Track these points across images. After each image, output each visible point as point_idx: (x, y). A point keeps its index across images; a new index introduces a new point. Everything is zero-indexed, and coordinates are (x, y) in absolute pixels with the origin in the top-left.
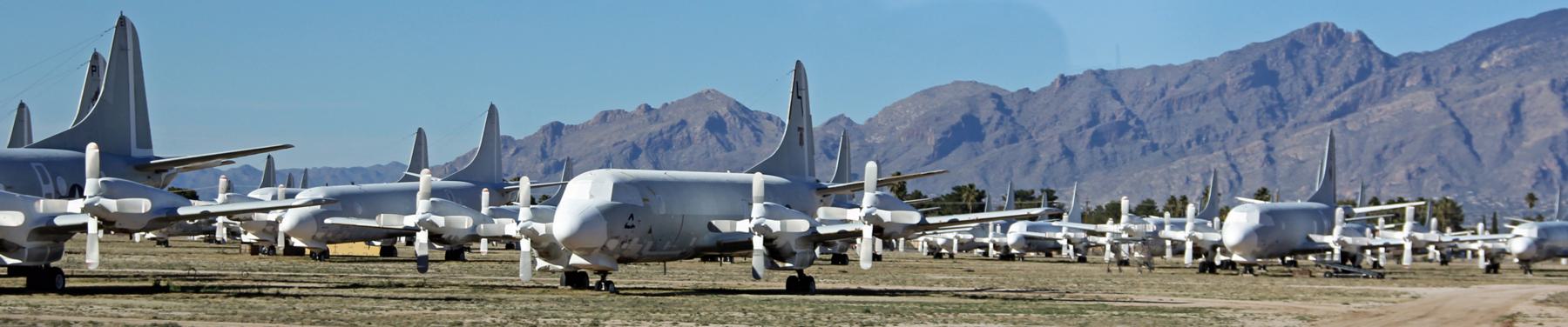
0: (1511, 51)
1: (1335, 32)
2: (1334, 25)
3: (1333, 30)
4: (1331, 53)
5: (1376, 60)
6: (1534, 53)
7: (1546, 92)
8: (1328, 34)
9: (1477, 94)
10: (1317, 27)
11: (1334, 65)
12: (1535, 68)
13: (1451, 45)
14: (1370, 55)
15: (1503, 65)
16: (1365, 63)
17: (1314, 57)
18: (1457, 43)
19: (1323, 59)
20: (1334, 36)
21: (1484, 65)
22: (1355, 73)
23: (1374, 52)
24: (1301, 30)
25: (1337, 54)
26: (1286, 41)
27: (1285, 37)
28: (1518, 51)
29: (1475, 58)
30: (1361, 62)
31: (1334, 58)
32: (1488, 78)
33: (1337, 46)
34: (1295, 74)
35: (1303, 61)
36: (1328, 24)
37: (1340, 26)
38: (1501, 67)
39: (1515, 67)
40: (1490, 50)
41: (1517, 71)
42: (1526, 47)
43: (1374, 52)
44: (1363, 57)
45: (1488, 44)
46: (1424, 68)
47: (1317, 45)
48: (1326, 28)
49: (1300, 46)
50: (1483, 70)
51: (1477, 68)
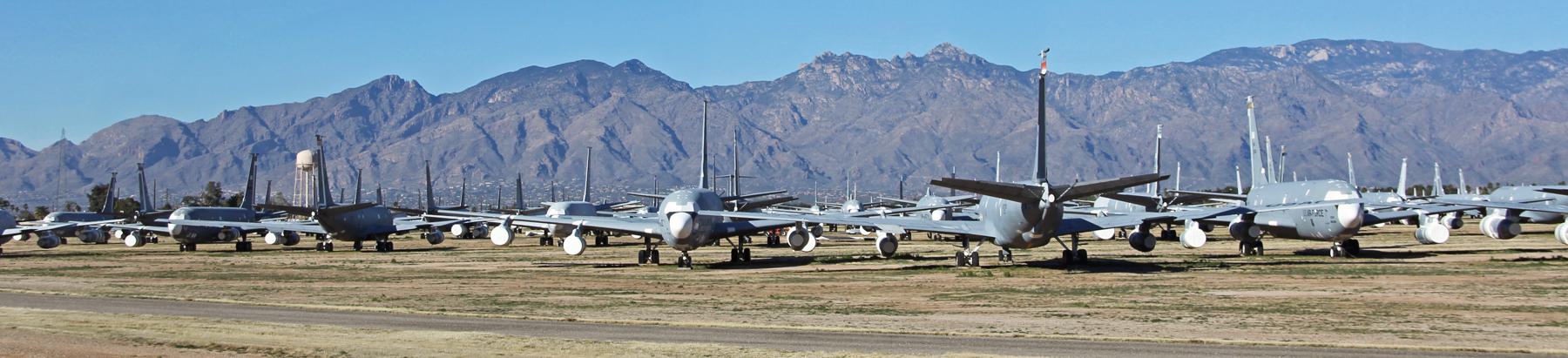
4: (398, 94)
5: (426, 99)
8: (396, 83)
9: (493, 119)
10: (388, 77)
11: (400, 102)
12: (525, 103)
13: (469, 89)
14: (422, 95)
16: (419, 100)
17: (387, 97)
20: (399, 84)
21: (491, 101)
22: (414, 106)
23: (424, 93)
24: (378, 80)
25: (401, 95)
26: (369, 87)
27: (368, 85)
28: (510, 93)
29: (484, 97)
30: (417, 99)
31: (399, 97)
32: (497, 109)
34: (376, 108)
35: (380, 100)
39: (513, 102)
40: (493, 91)
42: (515, 90)
43: (424, 93)
44: (418, 96)
45: (491, 89)
46: (459, 104)
48: (393, 79)
49: (380, 91)
50: (493, 104)
51: (486, 103)
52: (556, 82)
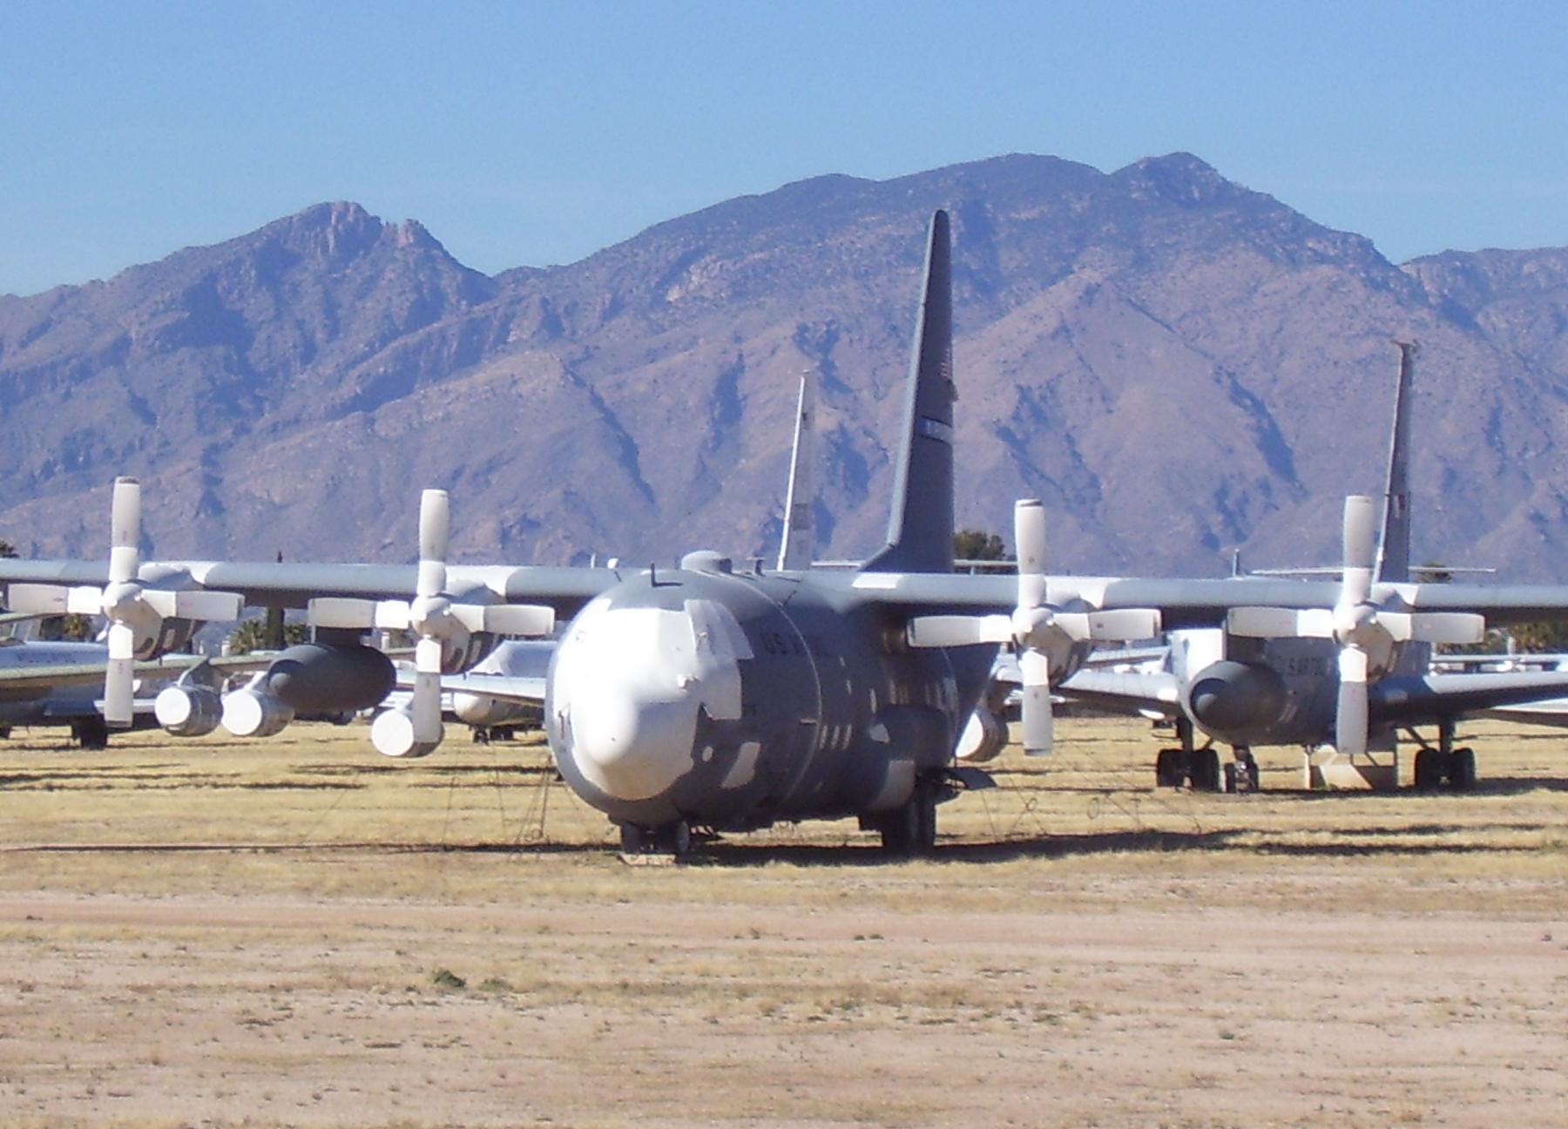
0: (728, 264)
1: (362, 225)
2: (359, 208)
3: (357, 219)
6: (769, 269)
7: (788, 353)
12: (769, 301)
15: (708, 294)
18: (617, 247)
19: (336, 281)
21: (674, 295)
32: (674, 323)
33: (366, 254)
36: (346, 205)
37: (371, 211)
38: (703, 299)
40: (684, 263)
41: (734, 307)
47: (325, 250)
48: (342, 217)
52: (889, 229)
